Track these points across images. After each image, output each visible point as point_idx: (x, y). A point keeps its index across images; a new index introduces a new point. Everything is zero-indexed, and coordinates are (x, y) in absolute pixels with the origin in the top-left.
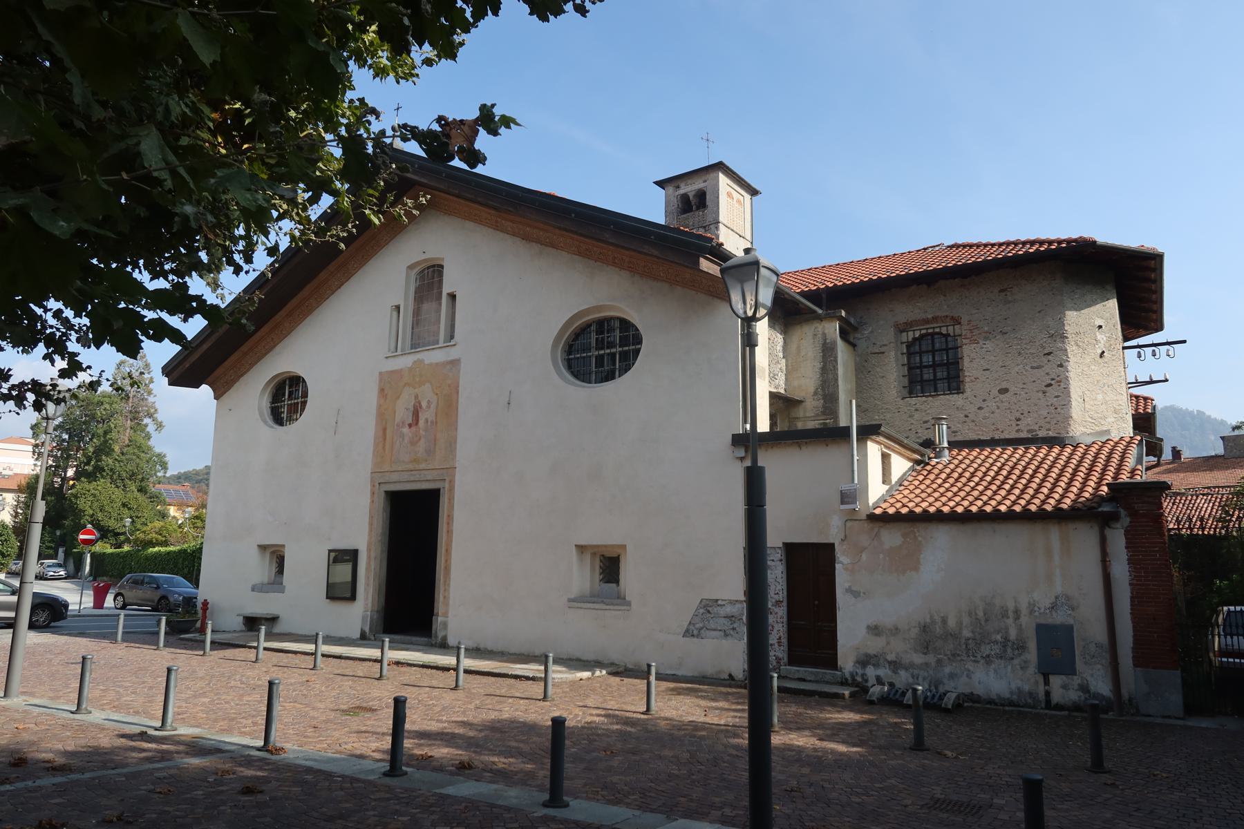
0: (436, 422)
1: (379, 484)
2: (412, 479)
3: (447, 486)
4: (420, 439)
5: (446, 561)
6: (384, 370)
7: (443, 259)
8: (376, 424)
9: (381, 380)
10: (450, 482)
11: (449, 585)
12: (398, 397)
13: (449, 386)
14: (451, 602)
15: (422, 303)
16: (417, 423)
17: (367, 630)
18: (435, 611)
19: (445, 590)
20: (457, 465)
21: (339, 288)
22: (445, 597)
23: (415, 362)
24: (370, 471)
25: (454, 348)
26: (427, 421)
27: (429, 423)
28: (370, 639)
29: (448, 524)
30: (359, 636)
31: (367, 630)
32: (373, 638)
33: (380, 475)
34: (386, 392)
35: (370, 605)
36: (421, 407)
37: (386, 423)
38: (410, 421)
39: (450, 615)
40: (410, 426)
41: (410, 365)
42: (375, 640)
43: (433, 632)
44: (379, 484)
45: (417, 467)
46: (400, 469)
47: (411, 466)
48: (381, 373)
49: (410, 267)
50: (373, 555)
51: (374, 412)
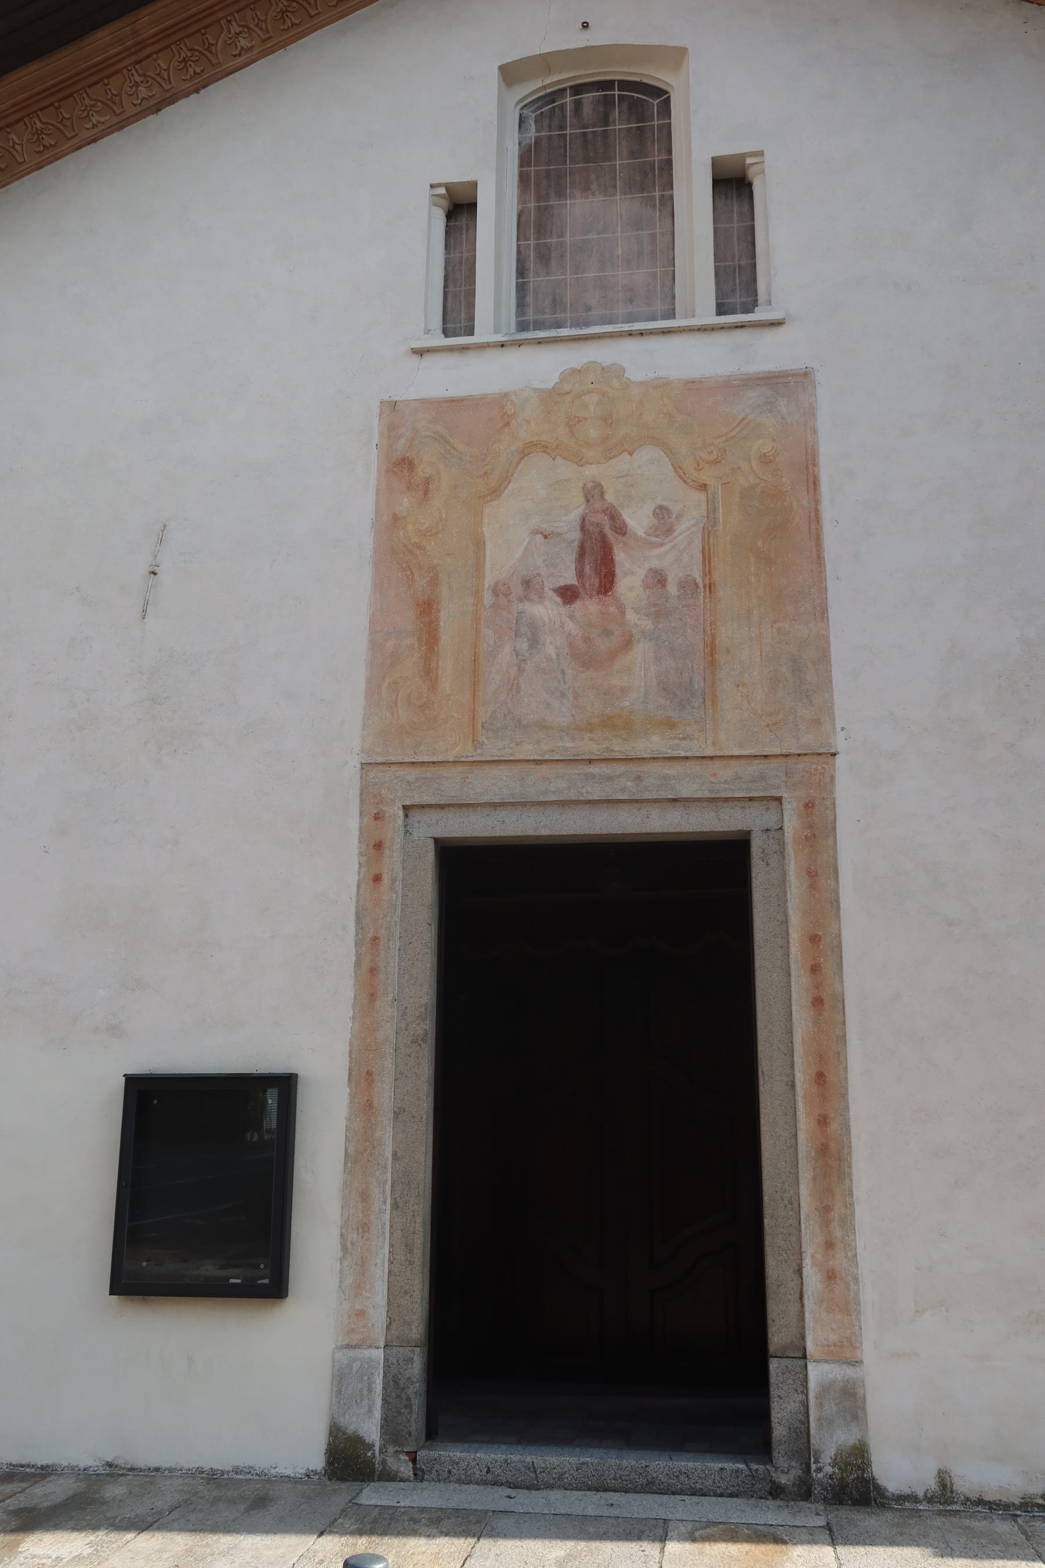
0: (711, 587)
1: (406, 808)
2: (595, 792)
3: (792, 824)
4: (628, 643)
5: (823, 1121)
6: (400, 395)
7: (676, 56)
8: (379, 586)
9: (391, 430)
10: (809, 805)
11: (847, 1222)
12: (495, 492)
13: (765, 460)
14: (868, 1295)
15: (561, 194)
16: (607, 582)
17: (371, 1430)
18: (777, 1336)
19: (829, 1245)
20: (840, 743)
21: (157, 109)
22: (831, 1276)
23: (574, 372)
24: (354, 763)
25: (769, 337)
26: (659, 579)
27: (672, 589)
28: (389, 1476)
29: (815, 969)
30: (316, 1459)
31: (371, 1430)
32: (406, 1469)
33: (412, 774)
34: (422, 470)
35: (378, 1317)
36: (621, 529)
37: (434, 583)
38: (569, 577)
39: (868, 1353)
40: (568, 594)
41: (550, 381)
42: (419, 1475)
43: (779, 1431)
44: (406, 808)
45: (620, 747)
46: (527, 751)
47: (588, 746)
48: (391, 407)
49: (510, 74)
50: (385, 1096)
51: (365, 539)
